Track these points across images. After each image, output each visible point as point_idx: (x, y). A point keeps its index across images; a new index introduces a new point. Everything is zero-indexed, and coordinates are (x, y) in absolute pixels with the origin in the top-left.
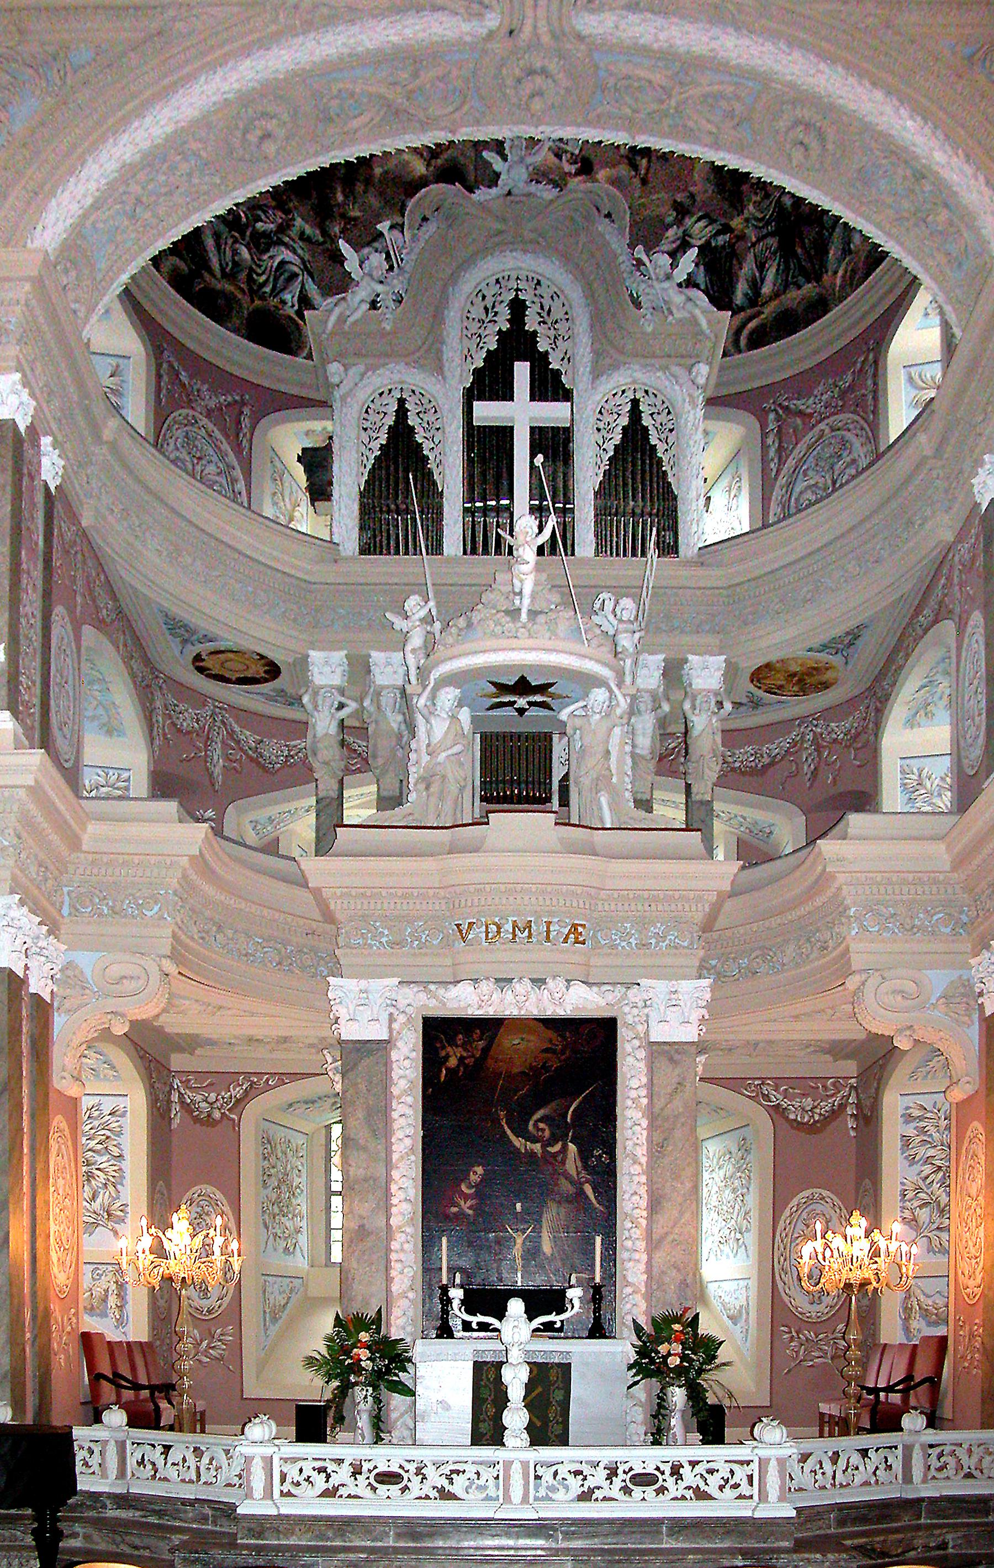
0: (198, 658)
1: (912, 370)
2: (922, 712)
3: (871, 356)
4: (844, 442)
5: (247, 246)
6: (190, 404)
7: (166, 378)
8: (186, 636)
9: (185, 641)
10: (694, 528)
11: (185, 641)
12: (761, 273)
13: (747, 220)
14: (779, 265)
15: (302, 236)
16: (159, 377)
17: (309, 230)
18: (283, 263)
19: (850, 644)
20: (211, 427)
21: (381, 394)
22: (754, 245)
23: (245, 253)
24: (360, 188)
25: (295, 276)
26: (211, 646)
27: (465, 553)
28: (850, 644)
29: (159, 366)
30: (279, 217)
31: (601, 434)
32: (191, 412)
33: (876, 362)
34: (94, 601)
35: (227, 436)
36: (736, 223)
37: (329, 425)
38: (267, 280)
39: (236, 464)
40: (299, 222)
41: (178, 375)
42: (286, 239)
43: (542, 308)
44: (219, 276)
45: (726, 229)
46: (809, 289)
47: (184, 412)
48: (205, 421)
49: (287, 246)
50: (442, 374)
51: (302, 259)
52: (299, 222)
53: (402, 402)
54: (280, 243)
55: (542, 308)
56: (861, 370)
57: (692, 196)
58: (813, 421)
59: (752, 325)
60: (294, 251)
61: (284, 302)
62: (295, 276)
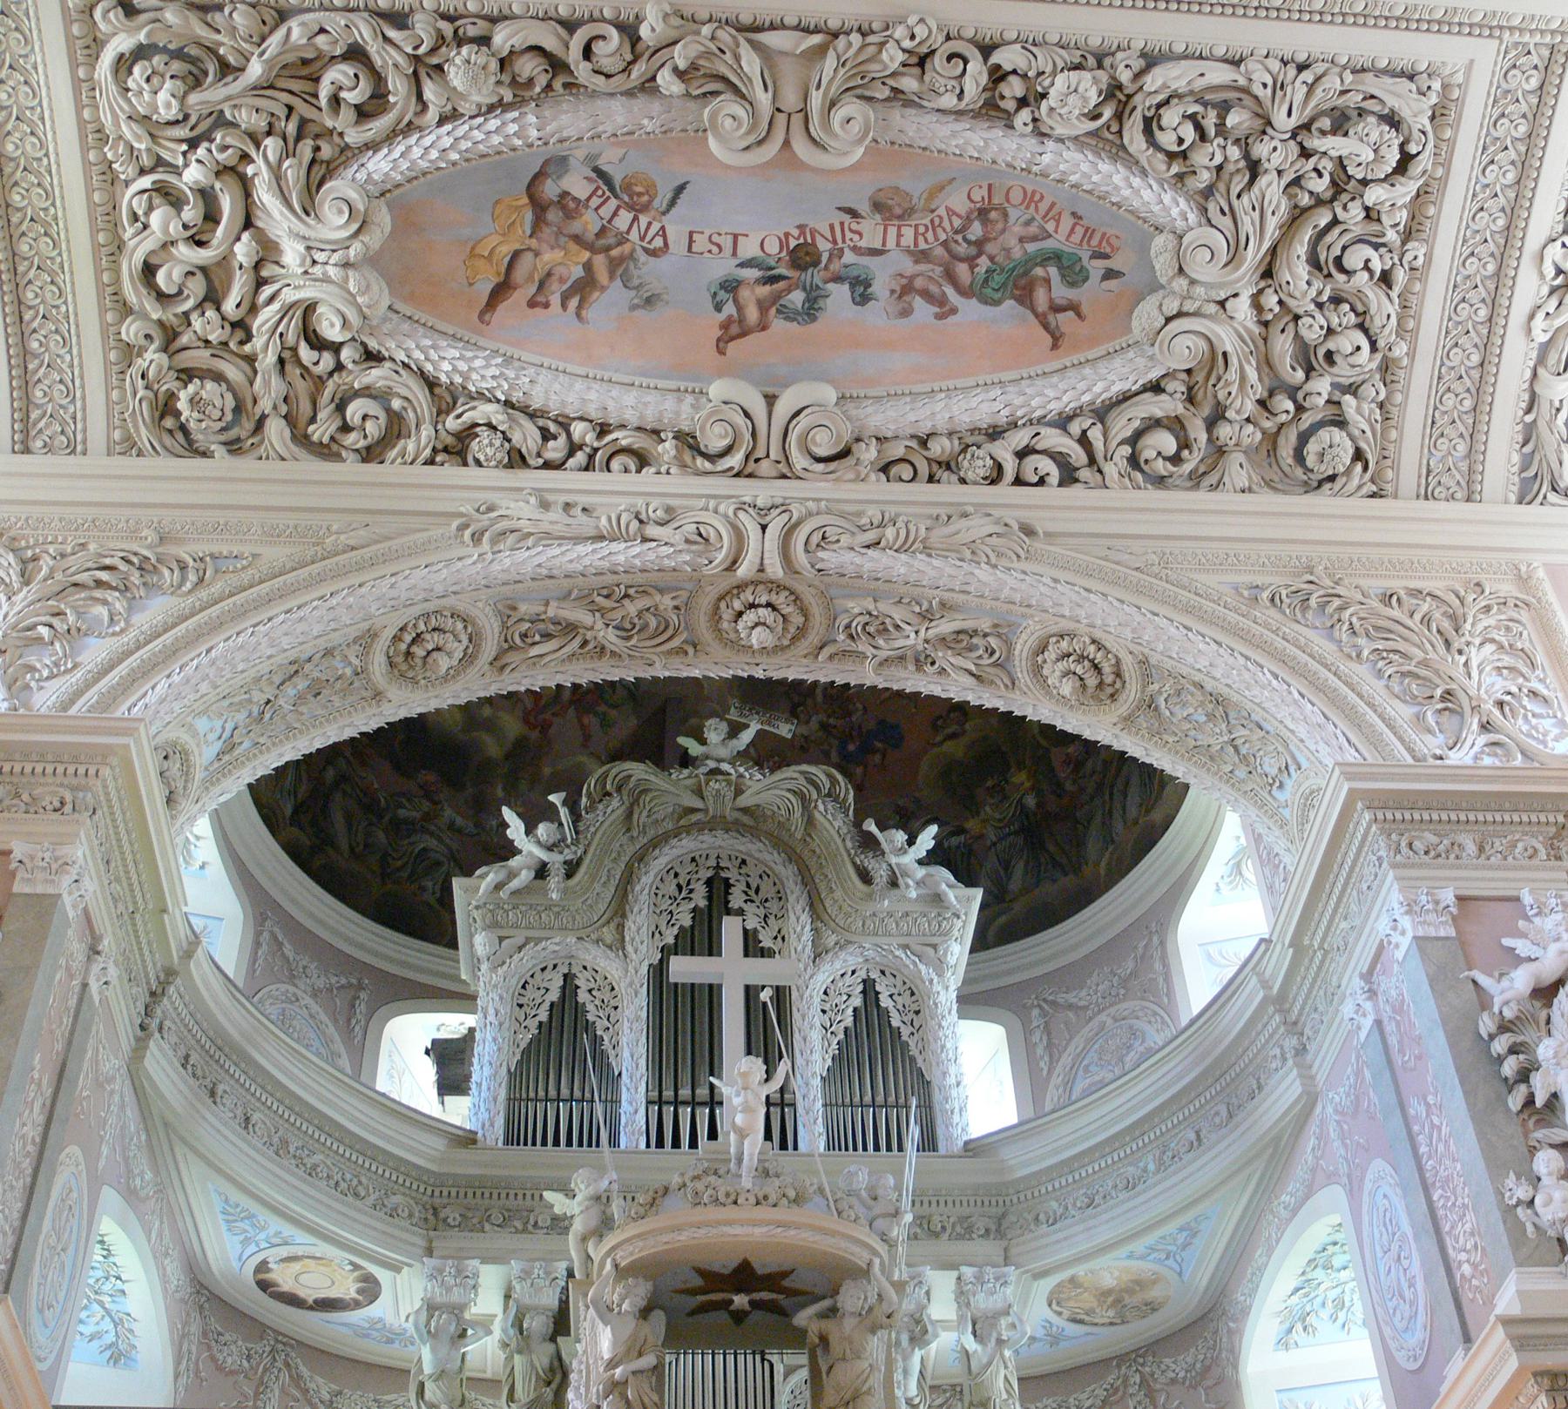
0: (263, 1267)
1: (1211, 949)
2: (1299, 1326)
3: (1155, 939)
4: (1133, 1033)
5: (385, 831)
6: (292, 978)
7: (265, 947)
8: (252, 1232)
9: (246, 1242)
10: (956, 1118)
11: (246, 1242)
12: (1006, 869)
13: (984, 821)
14: (1026, 866)
15: (451, 826)
16: (257, 944)
17: (459, 821)
18: (424, 849)
19: (1185, 1246)
20: (315, 1008)
21: (543, 970)
22: (994, 844)
23: (381, 836)
24: (523, 786)
25: (438, 864)
26: (284, 1252)
27: (648, 1146)
28: (1185, 1246)
29: (258, 934)
30: (426, 806)
31: (826, 1017)
32: (292, 989)
33: (1162, 943)
34: (126, 1159)
35: (336, 1021)
36: (972, 825)
37: (470, 1020)
38: (403, 866)
39: (342, 1050)
40: (448, 812)
41: (280, 945)
42: (433, 828)
43: (748, 886)
44: (346, 855)
45: (960, 831)
46: (1069, 881)
47: (283, 987)
48: (308, 1000)
49: (432, 834)
50: (624, 949)
51: (450, 849)
52: (448, 812)
53: (567, 977)
54: (424, 830)
55: (748, 886)
56: (1142, 957)
57: (917, 801)
58: (1089, 1013)
59: (1003, 919)
60: (440, 839)
61: (423, 889)
62: (438, 864)
